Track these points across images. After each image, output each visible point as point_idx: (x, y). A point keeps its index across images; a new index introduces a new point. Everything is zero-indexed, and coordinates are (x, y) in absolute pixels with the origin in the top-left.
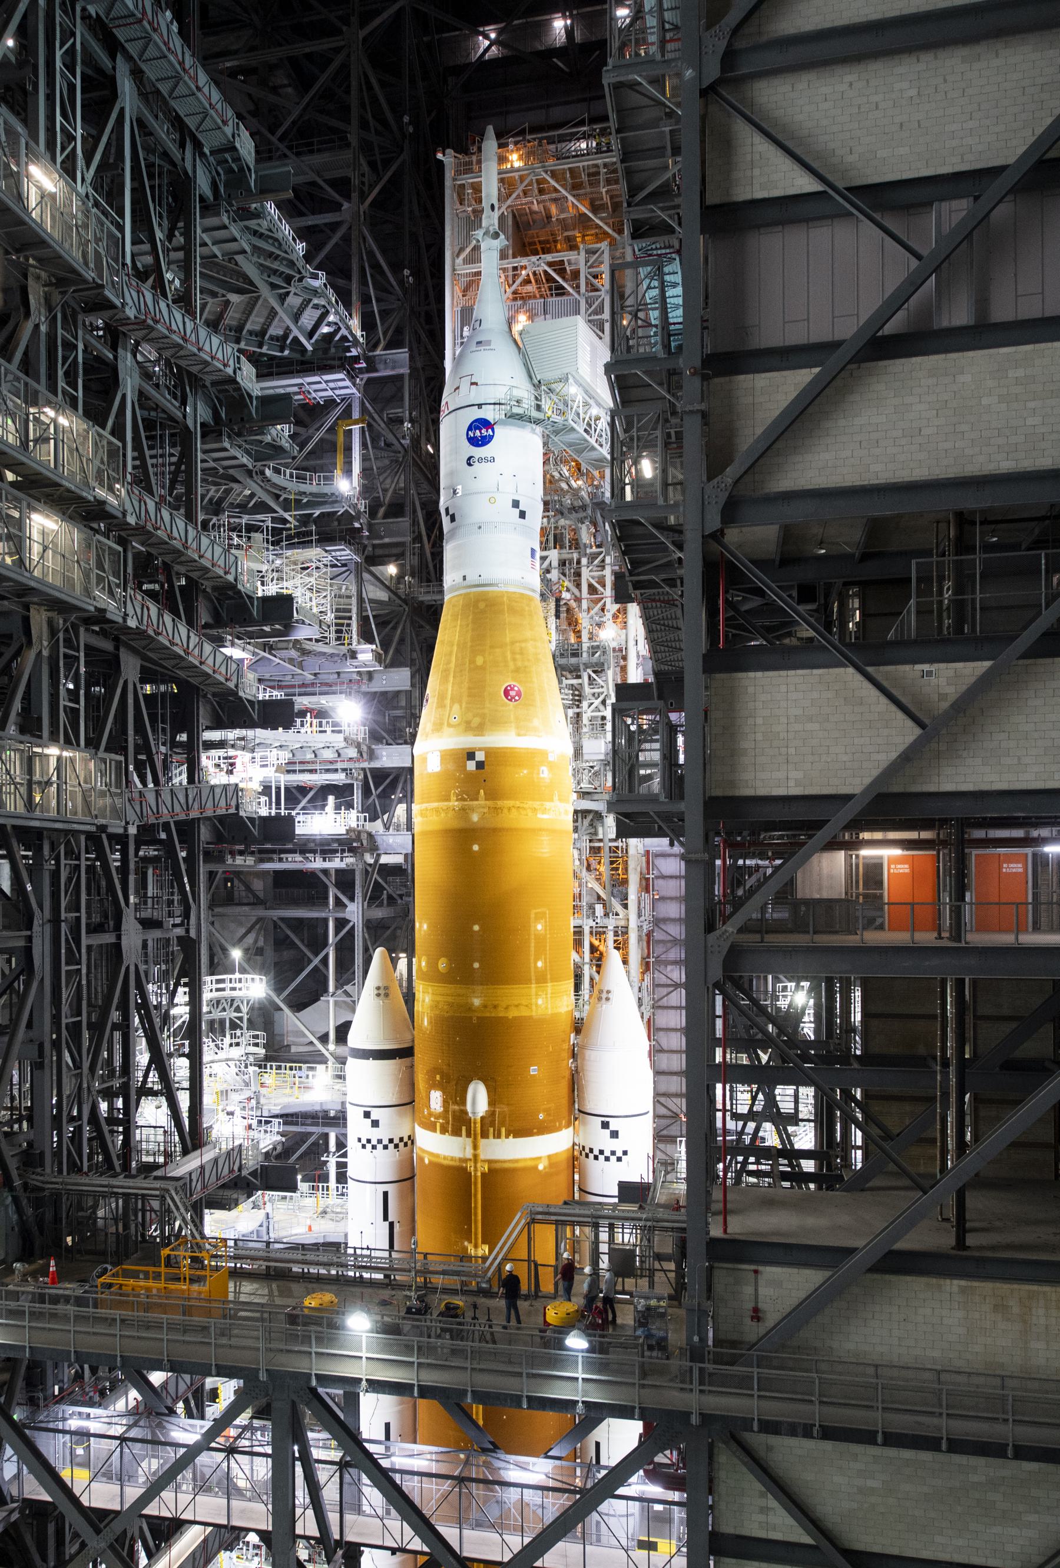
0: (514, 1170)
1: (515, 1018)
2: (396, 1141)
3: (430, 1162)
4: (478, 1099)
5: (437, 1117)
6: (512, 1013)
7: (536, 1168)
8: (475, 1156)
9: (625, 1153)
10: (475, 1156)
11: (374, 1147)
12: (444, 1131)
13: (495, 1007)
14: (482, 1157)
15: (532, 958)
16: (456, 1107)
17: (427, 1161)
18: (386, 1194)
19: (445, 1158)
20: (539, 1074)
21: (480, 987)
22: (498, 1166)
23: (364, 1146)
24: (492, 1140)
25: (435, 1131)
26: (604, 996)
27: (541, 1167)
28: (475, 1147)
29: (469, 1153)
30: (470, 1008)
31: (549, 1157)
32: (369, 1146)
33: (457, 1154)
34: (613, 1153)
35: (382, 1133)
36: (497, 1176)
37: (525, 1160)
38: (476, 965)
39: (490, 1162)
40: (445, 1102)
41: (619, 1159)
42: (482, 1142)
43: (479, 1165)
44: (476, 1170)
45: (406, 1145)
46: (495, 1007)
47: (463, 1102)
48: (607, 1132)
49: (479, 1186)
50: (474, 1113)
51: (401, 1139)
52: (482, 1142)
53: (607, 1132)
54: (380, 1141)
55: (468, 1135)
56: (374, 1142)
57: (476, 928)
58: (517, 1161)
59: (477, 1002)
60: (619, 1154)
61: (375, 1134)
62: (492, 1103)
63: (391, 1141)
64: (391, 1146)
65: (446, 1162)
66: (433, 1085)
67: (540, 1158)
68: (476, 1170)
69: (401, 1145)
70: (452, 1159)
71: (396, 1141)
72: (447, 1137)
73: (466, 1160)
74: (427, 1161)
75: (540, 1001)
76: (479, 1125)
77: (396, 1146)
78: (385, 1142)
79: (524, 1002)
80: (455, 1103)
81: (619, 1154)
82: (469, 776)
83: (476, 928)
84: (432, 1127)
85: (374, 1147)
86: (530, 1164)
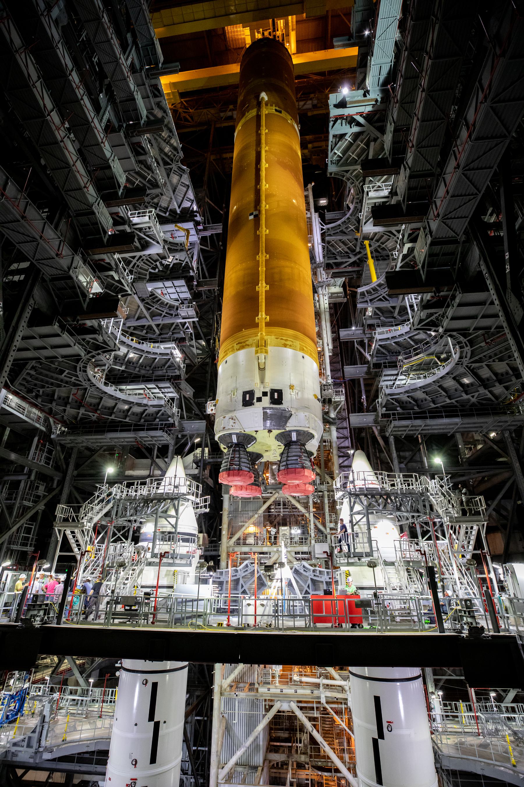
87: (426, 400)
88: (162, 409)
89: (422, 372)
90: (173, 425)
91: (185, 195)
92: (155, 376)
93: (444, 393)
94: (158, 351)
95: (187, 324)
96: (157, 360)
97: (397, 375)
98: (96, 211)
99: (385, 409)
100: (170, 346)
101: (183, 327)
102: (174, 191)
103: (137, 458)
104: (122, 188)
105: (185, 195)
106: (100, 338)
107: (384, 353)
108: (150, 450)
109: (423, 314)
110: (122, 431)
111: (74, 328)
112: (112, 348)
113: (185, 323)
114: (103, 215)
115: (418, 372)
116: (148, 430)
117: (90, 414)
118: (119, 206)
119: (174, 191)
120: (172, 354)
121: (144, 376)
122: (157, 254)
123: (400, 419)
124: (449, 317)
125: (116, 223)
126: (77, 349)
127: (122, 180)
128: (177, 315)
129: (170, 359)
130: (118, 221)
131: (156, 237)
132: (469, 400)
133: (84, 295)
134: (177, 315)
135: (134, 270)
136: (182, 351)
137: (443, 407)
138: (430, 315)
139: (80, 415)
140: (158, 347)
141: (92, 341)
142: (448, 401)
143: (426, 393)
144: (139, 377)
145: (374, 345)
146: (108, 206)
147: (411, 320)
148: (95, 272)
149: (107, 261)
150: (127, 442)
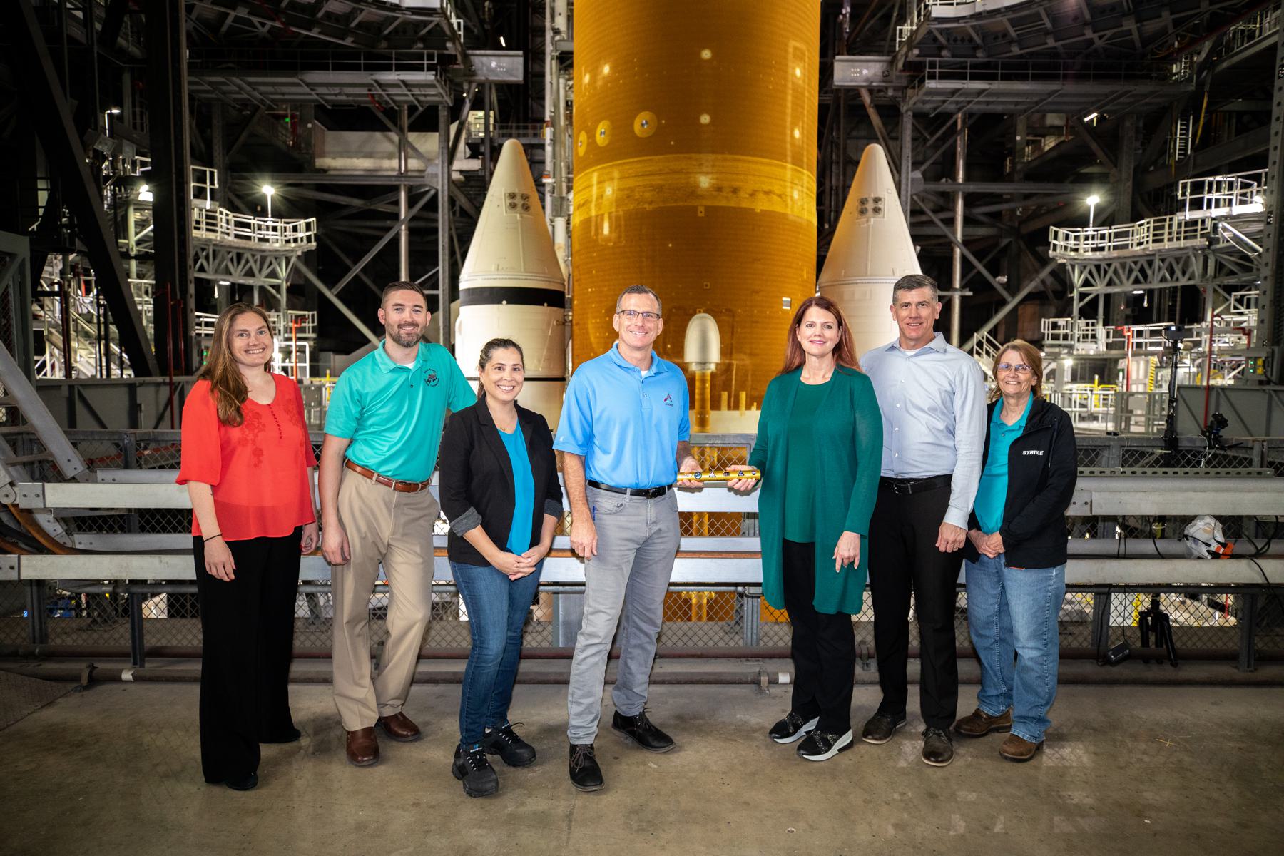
87: (1005, 35)
88: (436, 19)
90: (452, 59)
93: (1049, 25)
99: (916, 52)
103: (330, 129)
108: (393, 115)
110: (338, 67)
116: (401, 68)
117: (255, 20)
123: (943, 77)
132: (1091, 42)
137: (1032, 54)
139: (229, 21)
142: (1051, 42)
143: (1014, 22)
150: (348, 95)
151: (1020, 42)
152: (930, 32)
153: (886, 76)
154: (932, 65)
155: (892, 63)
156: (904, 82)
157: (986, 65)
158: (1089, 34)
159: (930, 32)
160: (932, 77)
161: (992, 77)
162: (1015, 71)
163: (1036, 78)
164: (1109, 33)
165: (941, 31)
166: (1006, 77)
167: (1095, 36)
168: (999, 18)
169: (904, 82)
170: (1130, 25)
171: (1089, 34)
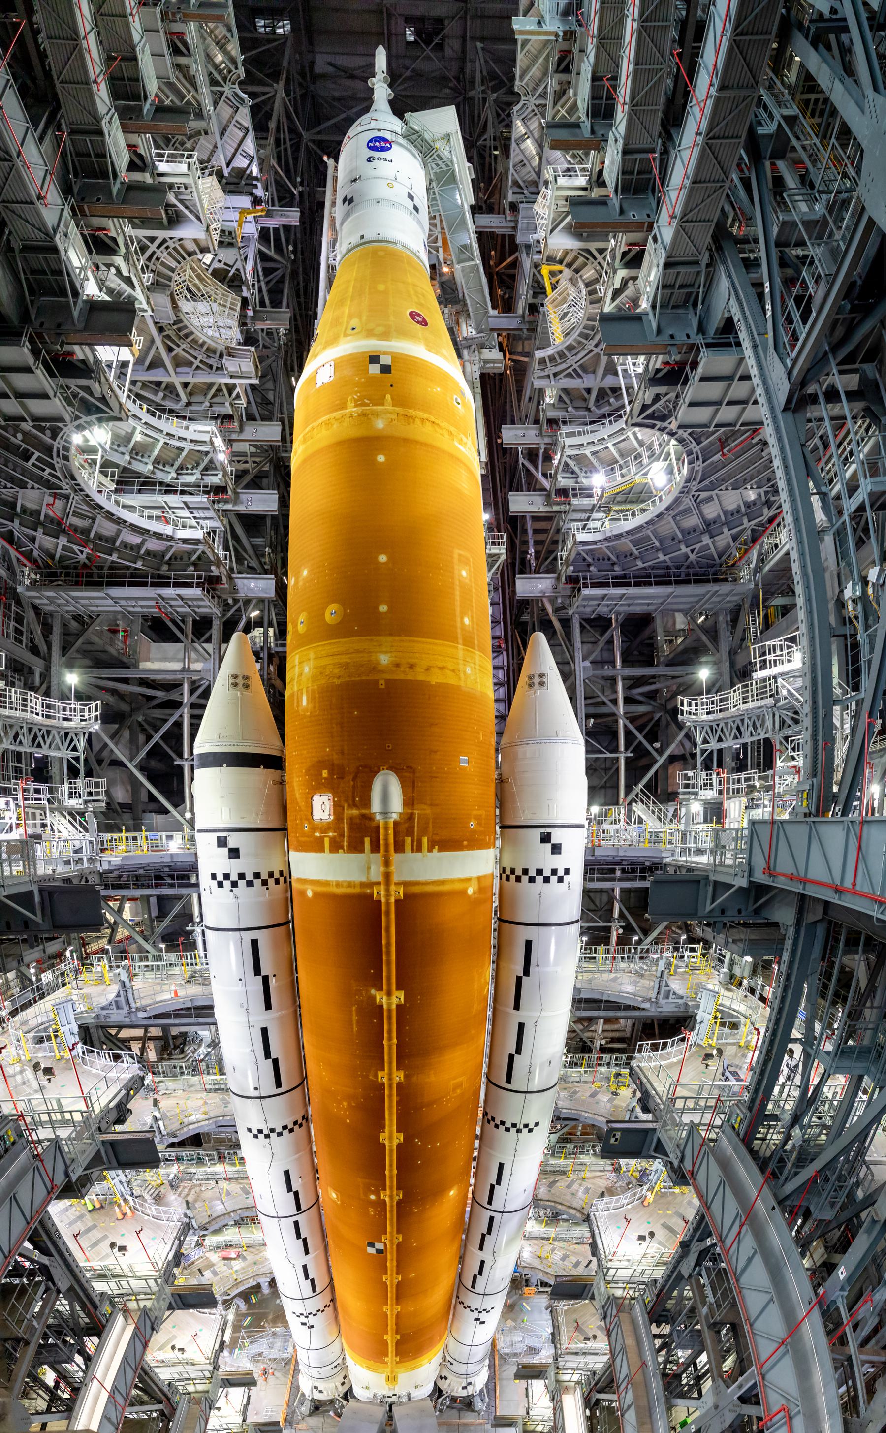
0: (437, 896)
1: (439, 685)
2: (264, 876)
3: (316, 894)
4: (388, 797)
5: (325, 828)
6: (435, 678)
7: (464, 892)
8: (387, 876)
9: (567, 871)
10: (387, 876)
11: (234, 884)
12: (336, 847)
13: (412, 666)
14: (395, 878)
15: (458, 610)
16: (355, 812)
17: (310, 894)
18: (255, 943)
19: (338, 884)
20: (469, 765)
21: (390, 638)
22: (416, 889)
23: (220, 885)
24: (409, 855)
25: (321, 850)
26: (537, 680)
27: (470, 891)
28: (387, 863)
29: (376, 873)
30: (374, 668)
31: (479, 879)
32: (227, 884)
33: (358, 877)
34: (554, 872)
35: (244, 865)
36: (415, 904)
37: (452, 881)
38: (383, 608)
39: (406, 884)
40: (338, 808)
41: (560, 880)
42: (395, 857)
43: (393, 888)
44: (388, 895)
45: (277, 882)
46: (412, 666)
47: (366, 802)
48: (548, 846)
49: (393, 916)
50: (385, 813)
51: (271, 875)
52: (395, 857)
53: (548, 846)
54: (242, 876)
55: (376, 848)
56: (234, 877)
57: (383, 558)
58: (443, 882)
59: (384, 659)
60: (561, 873)
61: (234, 867)
62: (408, 802)
63: (257, 875)
64: (258, 882)
65: (339, 891)
66: (318, 787)
67: (469, 880)
68: (388, 895)
69: (271, 882)
70: (350, 884)
71: (264, 876)
72: (341, 855)
73: (371, 885)
74: (310, 894)
75: (468, 671)
76: (391, 832)
77: (265, 883)
78: (249, 876)
79: (450, 665)
80: (354, 805)
81: (561, 873)
82: (372, 380)
83: (383, 558)
84: (317, 846)
85: (234, 884)
86: (458, 886)
89: (628, 507)
91: (239, 145)
92: (183, 485)
94: (188, 435)
95: (238, 389)
96: (184, 454)
97: (592, 511)
98: (106, 131)
100: (208, 428)
101: (230, 394)
102: (222, 134)
104: (149, 102)
105: (239, 145)
106: (96, 388)
107: (573, 472)
109: (648, 396)
111: (55, 360)
112: (115, 414)
113: (234, 386)
114: (117, 143)
115: (623, 507)
118: (139, 133)
119: (222, 134)
120: (212, 443)
121: (161, 484)
122: (195, 241)
124: (687, 401)
125: (132, 167)
126: (56, 406)
127: (152, 86)
128: (220, 368)
129: (207, 453)
130: (138, 163)
131: (195, 205)
133: (76, 294)
134: (220, 368)
135: (152, 266)
136: (229, 442)
137: (653, 568)
138: (657, 398)
140: (187, 428)
141: (82, 394)
142: (662, 557)
144: (154, 484)
145: (558, 457)
146: (125, 130)
147: (628, 408)
148: (90, 252)
149: (113, 234)
151: (641, 557)
152: (579, 554)
153: (555, 588)
154: (585, 578)
155: (558, 579)
156: (569, 593)
157: (624, 576)
158: (684, 549)
159: (579, 554)
160: (585, 586)
161: (628, 585)
162: (642, 580)
163: (657, 583)
164: (698, 546)
165: (587, 552)
166: (637, 584)
167: (688, 550)
168: (623, 540)
169: (569, 593)
170: (706, 540)
171: (684, 549)
